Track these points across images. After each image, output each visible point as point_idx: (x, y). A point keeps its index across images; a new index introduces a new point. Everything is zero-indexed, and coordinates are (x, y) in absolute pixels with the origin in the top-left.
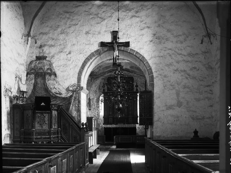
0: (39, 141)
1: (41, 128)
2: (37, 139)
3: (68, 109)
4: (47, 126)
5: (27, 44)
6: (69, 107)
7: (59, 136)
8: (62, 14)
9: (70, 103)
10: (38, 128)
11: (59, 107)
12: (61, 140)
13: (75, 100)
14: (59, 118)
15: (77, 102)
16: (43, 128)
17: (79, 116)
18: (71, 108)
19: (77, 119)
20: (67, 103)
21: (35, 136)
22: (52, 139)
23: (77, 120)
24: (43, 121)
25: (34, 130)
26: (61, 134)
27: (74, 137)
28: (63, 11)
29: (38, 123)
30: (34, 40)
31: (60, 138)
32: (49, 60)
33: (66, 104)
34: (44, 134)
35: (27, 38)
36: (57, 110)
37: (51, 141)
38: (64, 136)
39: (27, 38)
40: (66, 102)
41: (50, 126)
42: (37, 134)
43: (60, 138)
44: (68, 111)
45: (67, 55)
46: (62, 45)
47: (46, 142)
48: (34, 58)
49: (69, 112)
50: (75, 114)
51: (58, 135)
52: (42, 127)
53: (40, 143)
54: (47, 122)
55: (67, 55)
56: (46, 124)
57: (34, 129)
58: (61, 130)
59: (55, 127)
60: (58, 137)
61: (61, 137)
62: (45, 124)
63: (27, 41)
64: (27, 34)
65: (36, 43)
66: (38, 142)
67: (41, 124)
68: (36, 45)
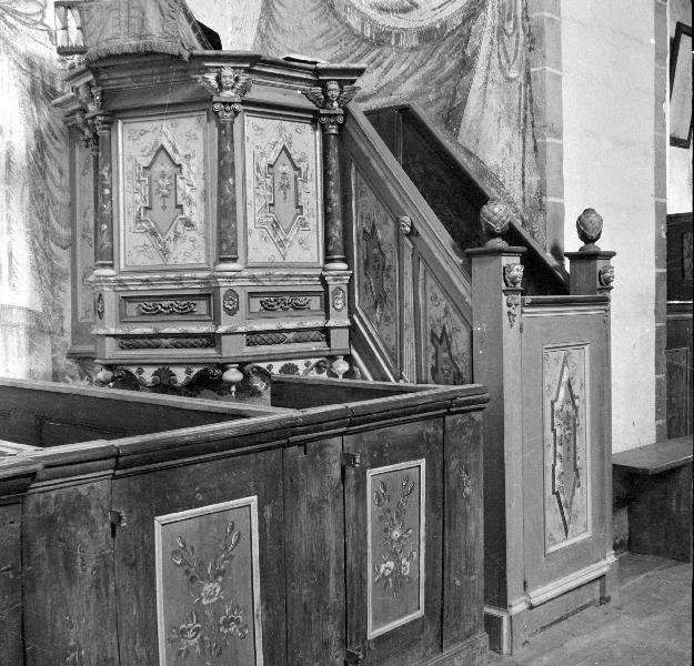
0: (141, 365)
1: (158, 261)
2: (130, 347)
3: (452, 116)
4: (200, 241)
6: (459, 95)
7: (331, 323)
9: (466, 65)
10: (142, 261)
11: (323, 84)
12: (349, 358)
13: (501, 31)
14: (332, 184)
15: (515, 43)
16: (171, 261)
17: (530, 158)
18: (473, 99)
19: (517, 184)
20: (451, 65)
23: (517, 195)
24: (170, 203)
25: (106, 279)
26: (351, 311)
27: (433, 335)
29: (138, 219)
33: (446, 79)
34: (183, 304)
36: (315, 119)
37: (223, 367)
38: (368, 330)
40: (441, 65)
41: (226, 247)
42: (132, 309)
43: (340, 340)
44: (457, 135)
47: (189, 372)
49: (463, 138)
50: (501, 145)
52: (165, 252)
53: (148, 375)
54: (196, 213)
56: (188, 224)
57: (111, 266)
60: (325, 331)
61: (353, 328)
62: (180, 228)
66: (134, 370)
67: (154, 233)
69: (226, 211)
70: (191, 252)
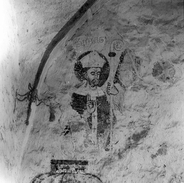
5: (27, 123)
8: (135, 27)
28: (139, 19)
30: (47, 109)
32: (95, 172)
35: (25, 104)
39: (25, 104)
45: (153, 156)
46: (137, 124)
48: (47, 166)
55: (153, 156)
63: (25, 115)
64: (28, 94)
65: (52, 118)
68: (52, 125)
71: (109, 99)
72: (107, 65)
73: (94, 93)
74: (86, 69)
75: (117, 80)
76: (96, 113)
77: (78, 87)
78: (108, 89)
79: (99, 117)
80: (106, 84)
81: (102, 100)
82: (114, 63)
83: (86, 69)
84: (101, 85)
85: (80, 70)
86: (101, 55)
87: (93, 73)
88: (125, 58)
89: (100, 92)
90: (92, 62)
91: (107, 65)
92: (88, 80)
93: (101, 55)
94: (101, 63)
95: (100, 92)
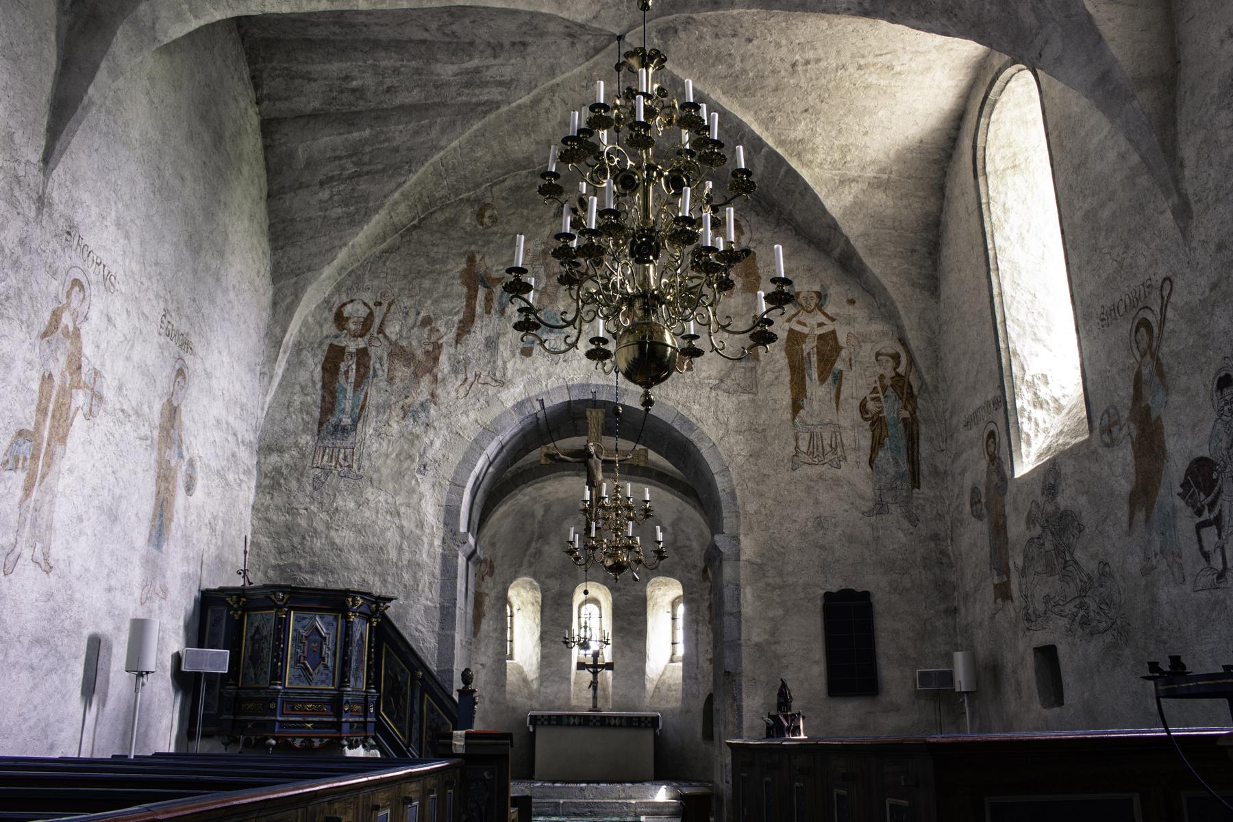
0: (294, 738)
1: (306, 685)
12: (375, 738)
21: (282, 714)
22: (345, 727)
25: (279, 691)
31: (371, 727)
43: (371, 727)
51: (366, 717)
52: (309, 681)
53: (297, 743)
54: (329, 661)
56: (326, 667)
58: (379, 698)
59: (358, 683)
60: (365, 723)
69: (345, 663)
70: (323, 683)
71: (372, 351)
72: (371, 314)
73: (353, 346)
74: (348, 319)
75: (381, 330)
76: (354, 366)
77: (336, 337)
78: (370, 340)
79: (357, 370)
80: (368, 336)
81: (363, 354)
82: (379, 313)
83: (348, 319)
84: (362, 336)
85: (340, 320)
86: (365, 304)
87: (355, 323)
88: (393, 308)
89: (361, 343)
90: (355, 311)
91: (371, 314)
92: (349, 330)
93: (365, 304)
94: (363, 312)
95: (361, 343)
